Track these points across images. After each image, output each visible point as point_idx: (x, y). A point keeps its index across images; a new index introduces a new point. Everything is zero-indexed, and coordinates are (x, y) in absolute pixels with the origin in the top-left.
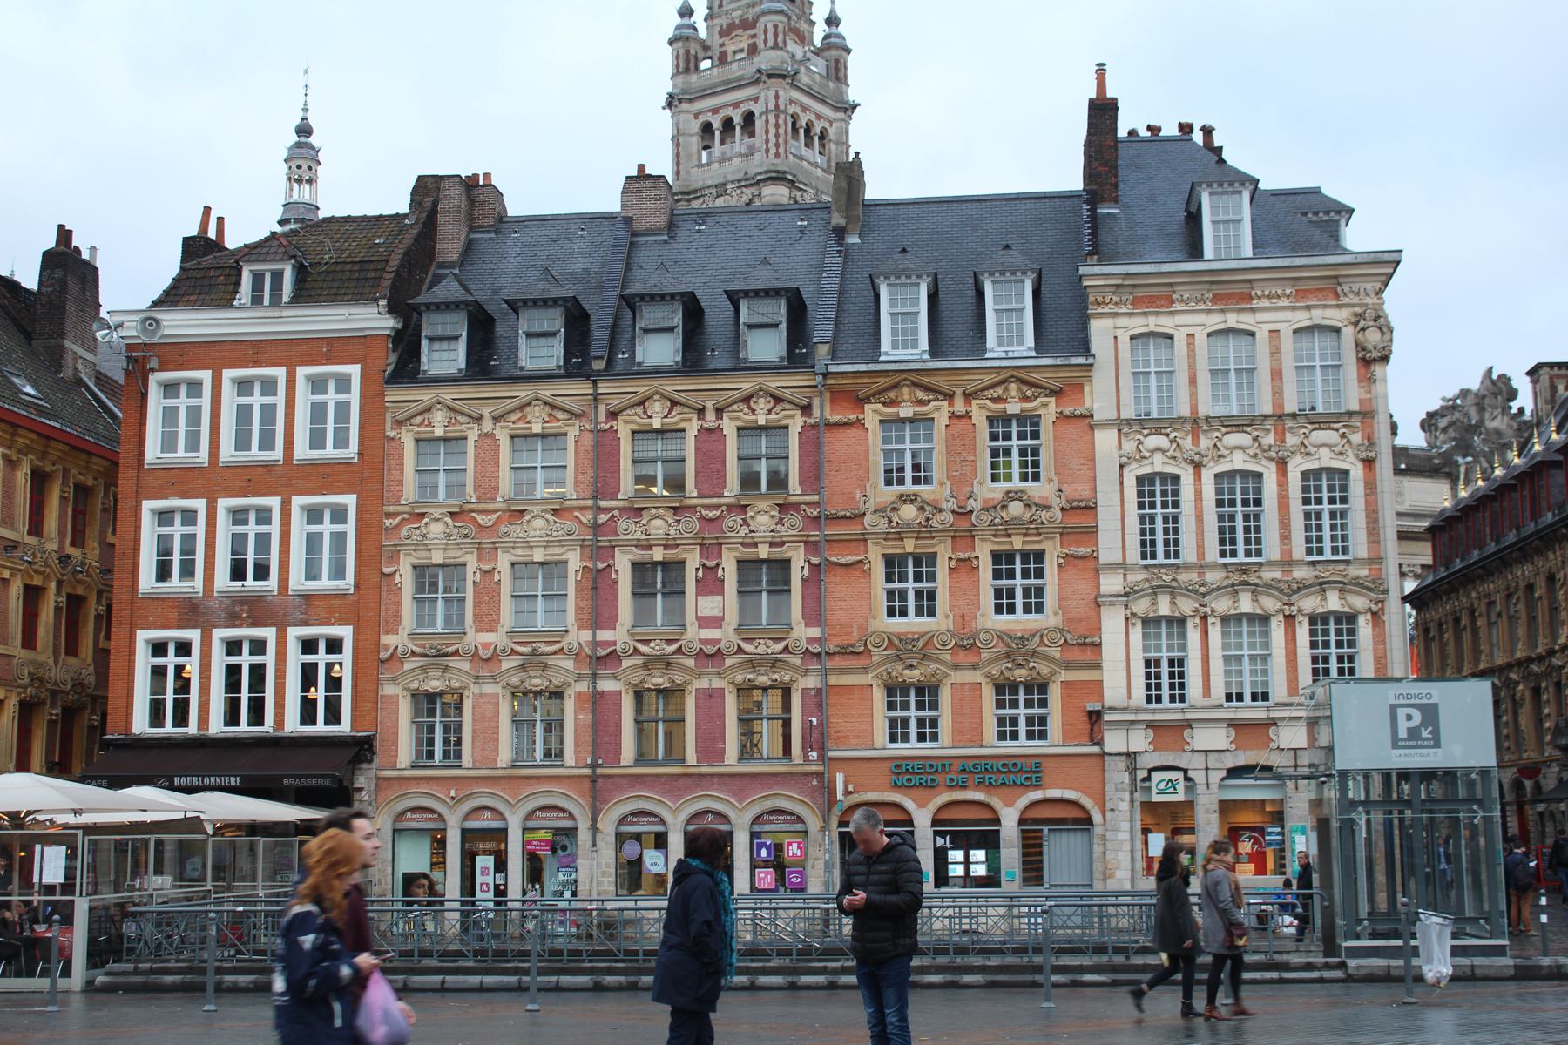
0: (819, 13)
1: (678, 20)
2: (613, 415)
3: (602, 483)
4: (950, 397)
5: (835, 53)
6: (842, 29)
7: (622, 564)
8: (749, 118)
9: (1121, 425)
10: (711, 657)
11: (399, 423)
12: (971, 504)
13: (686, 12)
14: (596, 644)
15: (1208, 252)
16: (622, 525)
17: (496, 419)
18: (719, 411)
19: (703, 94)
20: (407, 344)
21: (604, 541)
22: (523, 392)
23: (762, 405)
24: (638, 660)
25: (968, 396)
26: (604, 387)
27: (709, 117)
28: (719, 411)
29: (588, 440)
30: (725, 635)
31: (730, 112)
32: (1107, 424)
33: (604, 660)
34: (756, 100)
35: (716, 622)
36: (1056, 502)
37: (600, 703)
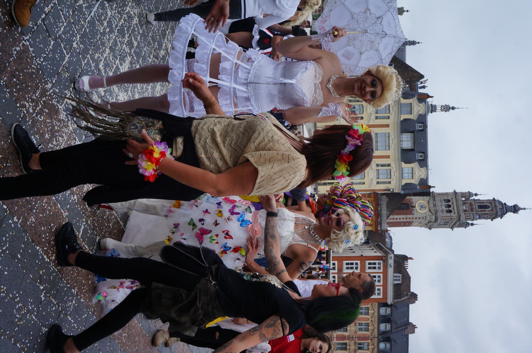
1: (474, 193)
2: (371, 339)
3: (359, 338)
5: (466, 225)
6: (470, 226)
7: (347, 341)
8: (450, 211)
11: (372, 305)
13: (476, 195)
14: (334, 338)
17: (372, 321)
19: (457, 200)
20: (385, 305)
22: (376, 326)
27: (451, 202)
29: (367, 336)
31: (452, 207)
34: (454, 213)
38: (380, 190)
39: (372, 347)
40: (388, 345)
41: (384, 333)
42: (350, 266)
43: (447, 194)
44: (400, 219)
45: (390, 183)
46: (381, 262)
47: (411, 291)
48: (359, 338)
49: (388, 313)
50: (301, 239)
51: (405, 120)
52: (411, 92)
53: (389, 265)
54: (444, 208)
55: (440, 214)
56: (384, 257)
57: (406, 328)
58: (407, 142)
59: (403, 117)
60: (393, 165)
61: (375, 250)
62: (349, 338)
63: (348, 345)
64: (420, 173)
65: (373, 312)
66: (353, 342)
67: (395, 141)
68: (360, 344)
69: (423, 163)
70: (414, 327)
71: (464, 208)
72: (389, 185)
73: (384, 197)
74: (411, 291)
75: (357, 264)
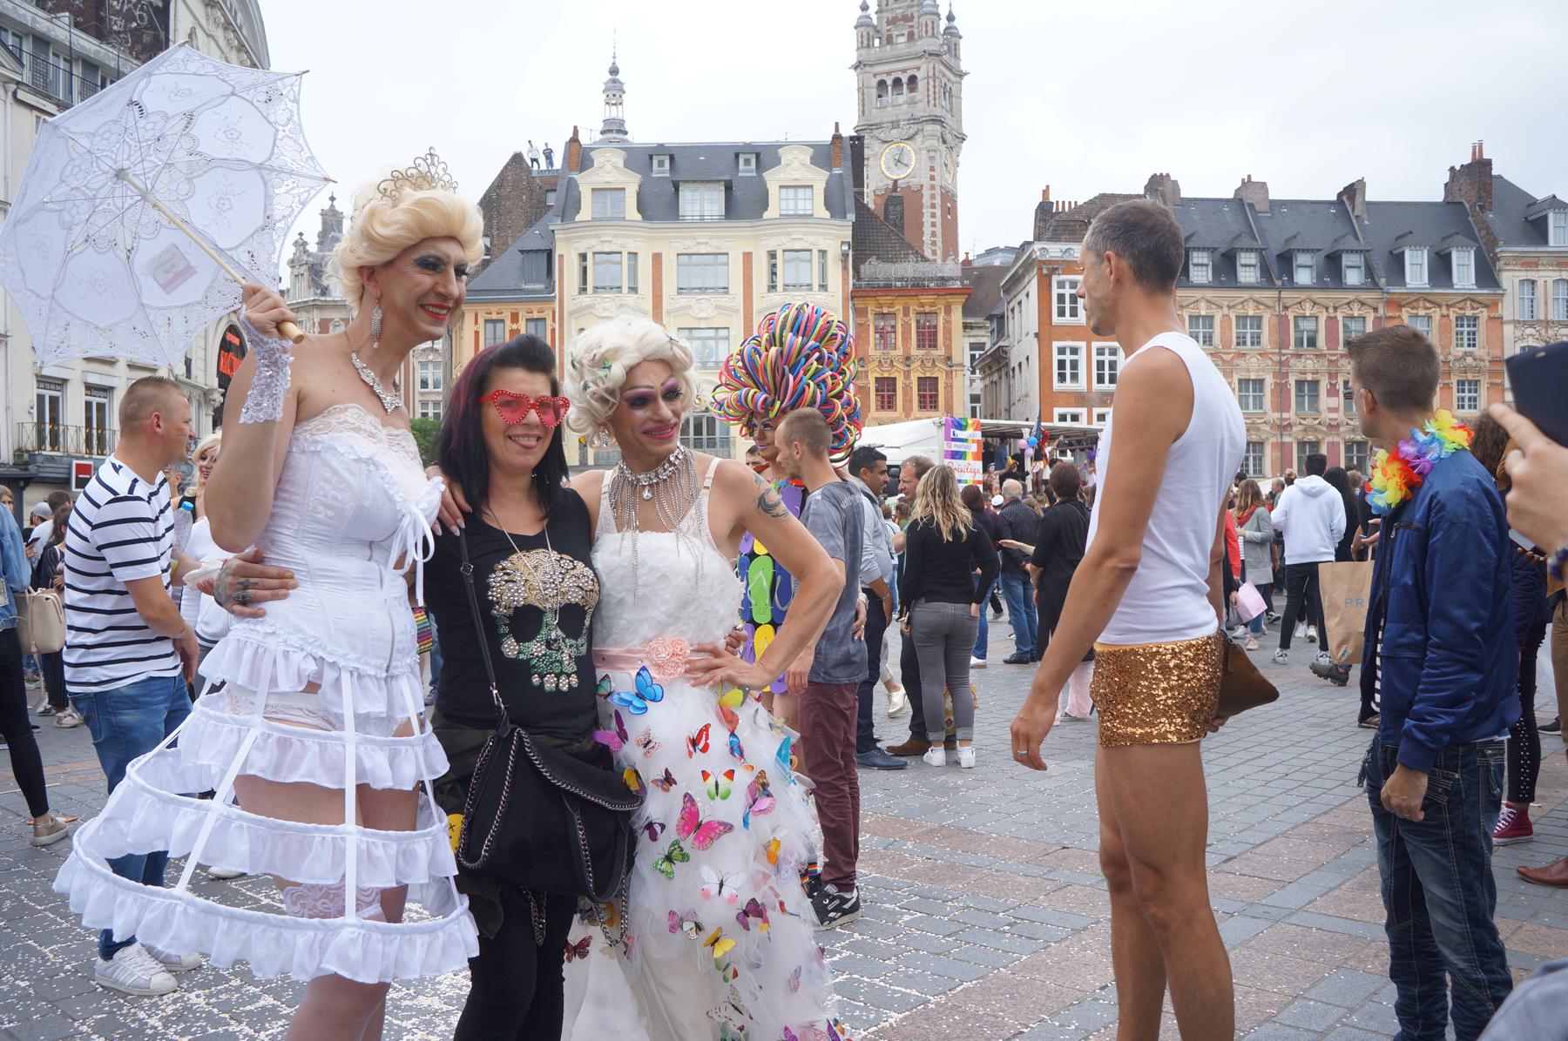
0: (944, 12)
1: (860, 13)
2: (1286, 308)
3: (1283, 344)
4: (1440, 306)
6: (955, 23)
7: (1292, 380)
8: (913, 79)
9: (1516, 322)
10: (1333, 427)
11: (1182, 307)
12: (1451, 358)
13: (865, 8)
14: (1282, 419)
15: (1551, 243)
16: (1292, 361)
18: (1335, 309)
19: (881, 62)
21: (1284, 369)
22: (1246, 295)
23: (1356, 306)
24: (1300, 428)
25: (1448, 306)
26: (1284, 294)
27: (884, 77)
28: (1335, 309)
29: (1275, 320)
30: (1340, 416)
32: (1509, 322)
33: (1283, 427)
35: (1335, 410)
36: (1487, 358)
37: (1283, 448)
38: (845, 279)
39: (1308, 305)
40: (1302, 259)
41: (1265, 270)
42: (1068, 371)
43: (861, 90)
44: (934, 225)
45: (823, 253)
46: (1055, 279)
47: (1142, 192)
48: (1283, 344)
49: (1205, 261)
50: (693, 511)
51: (640, 209)
52: (562, 189)
53: (1067, 257)
54: (901, 99)
55: (921, 110)
56: (1040, 269)
57: (1251, 206)
58: (701, 202)
59: (632, 213)
60: (772, 244)
61: (1022, 296)
62: (1282, 375)
63: (1302, 377)
64: (796, 168)
65: (1203, 305)
66: (1292, 361)
67: (702, 236)
68: (1299, 342)
69: (764, 156)
70: (1247, 183)
71: (902, 39)
72: (830, 256)
73: (865, 269)
74: (1142, 192)
75: (1062, 351)
